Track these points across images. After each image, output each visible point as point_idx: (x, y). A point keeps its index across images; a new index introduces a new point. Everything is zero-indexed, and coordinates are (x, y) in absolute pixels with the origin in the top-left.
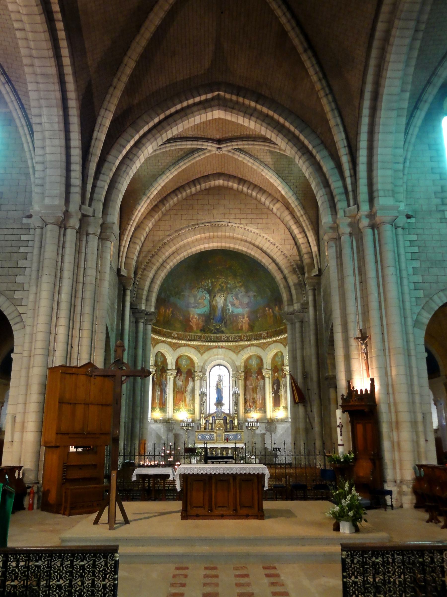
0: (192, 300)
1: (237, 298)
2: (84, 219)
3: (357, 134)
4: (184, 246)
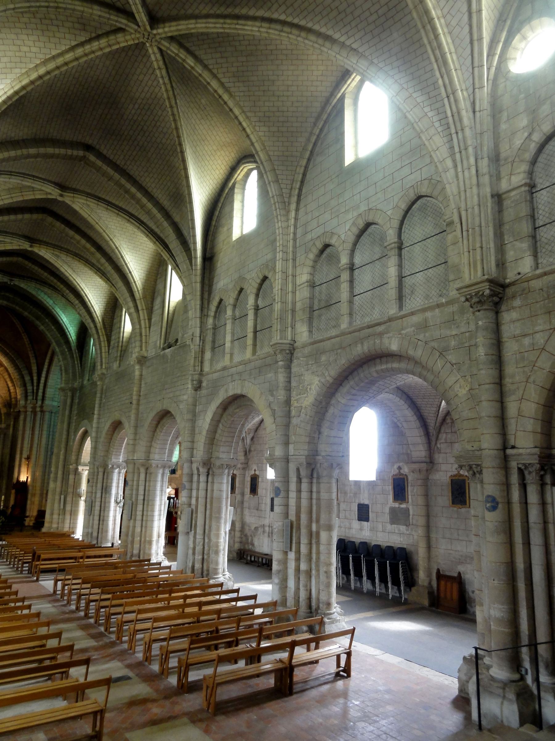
3: (42, 370)
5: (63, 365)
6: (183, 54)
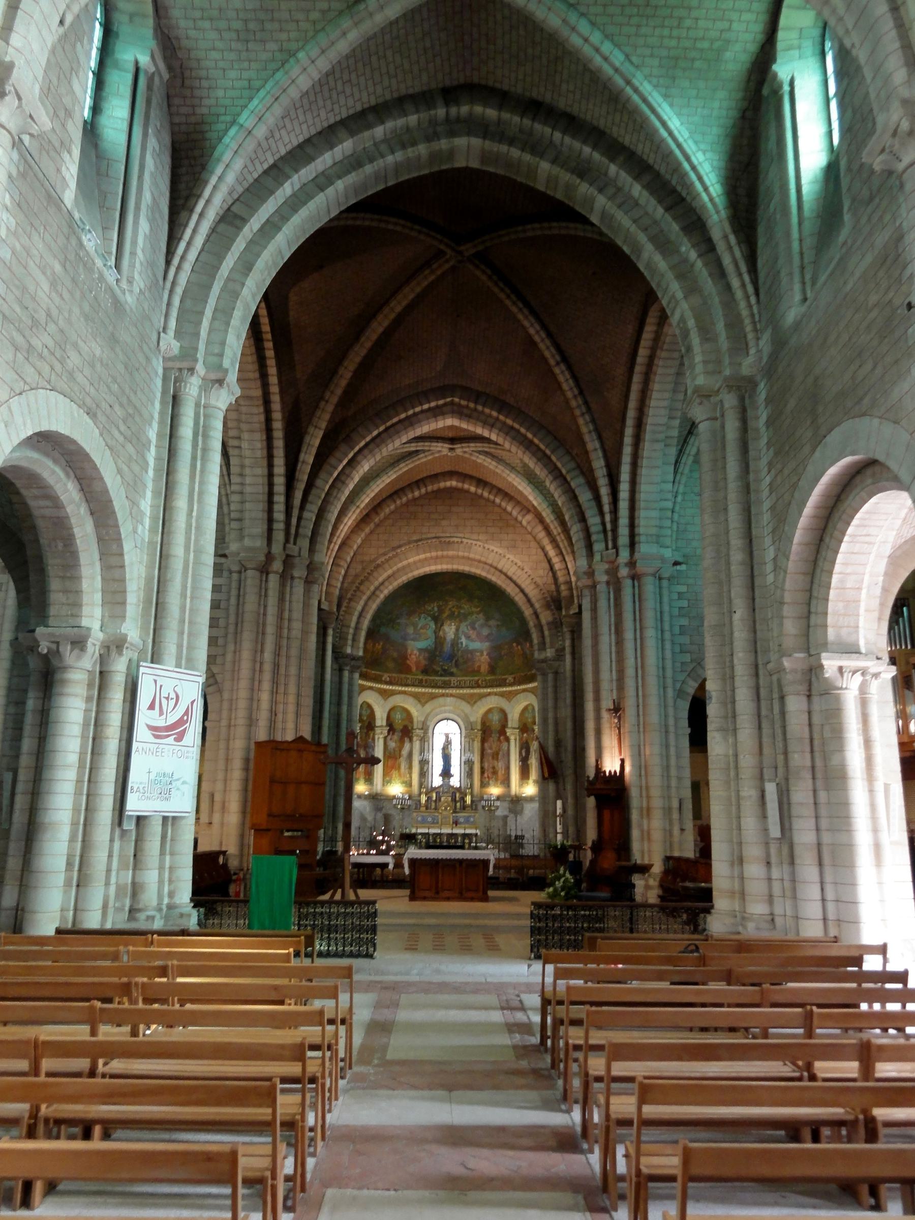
0: (410, 630)
1: (474, 628)
2: (288, 561)
4: (404, 568)
5: (688, 314)
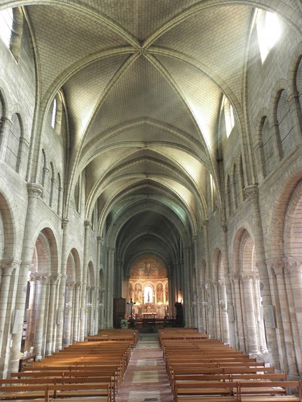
0: (140, 266)
6: (161, 51)
